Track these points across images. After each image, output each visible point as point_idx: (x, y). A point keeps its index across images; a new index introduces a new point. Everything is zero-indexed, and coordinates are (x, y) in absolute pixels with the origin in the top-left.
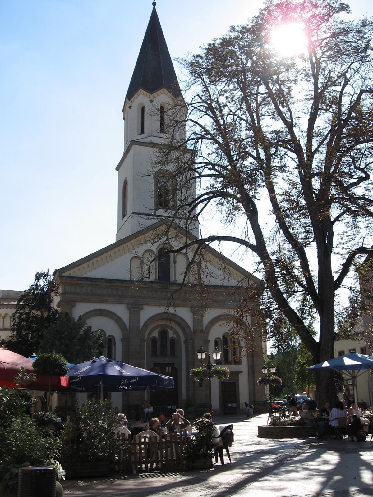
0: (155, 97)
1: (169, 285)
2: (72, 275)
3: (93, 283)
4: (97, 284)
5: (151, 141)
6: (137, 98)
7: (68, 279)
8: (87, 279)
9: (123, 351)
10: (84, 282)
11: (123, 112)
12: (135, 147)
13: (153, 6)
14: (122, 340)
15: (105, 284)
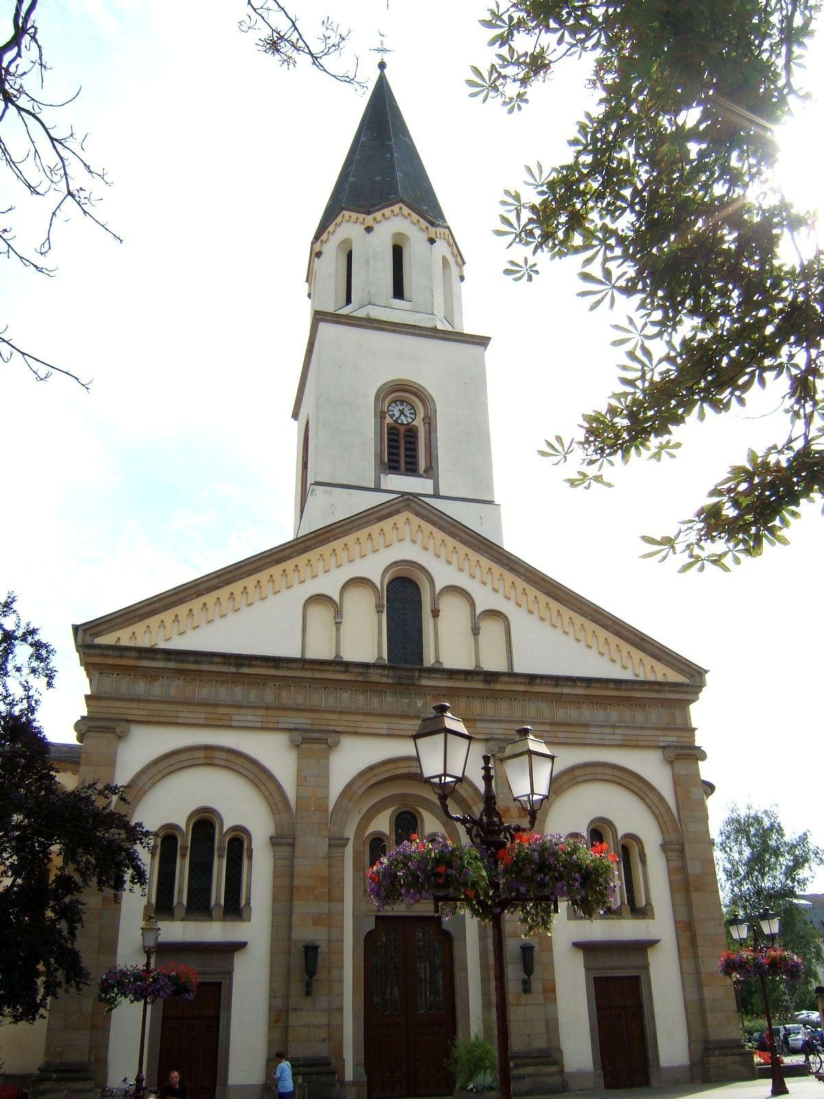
0: (377, 222)
1: (417, 674)
2: (125, 642)
3: (187, 666)
4: (201, 671)
5: (368, 314)
6: (334, 231)
7: (110, 652)
8: (169, 654)
9: (276, 876)
10: (161, 664)
11: (307, 281)
12: (323, 326)
13: (379, 72)
14: (275, 841)
15: (225, 669)
